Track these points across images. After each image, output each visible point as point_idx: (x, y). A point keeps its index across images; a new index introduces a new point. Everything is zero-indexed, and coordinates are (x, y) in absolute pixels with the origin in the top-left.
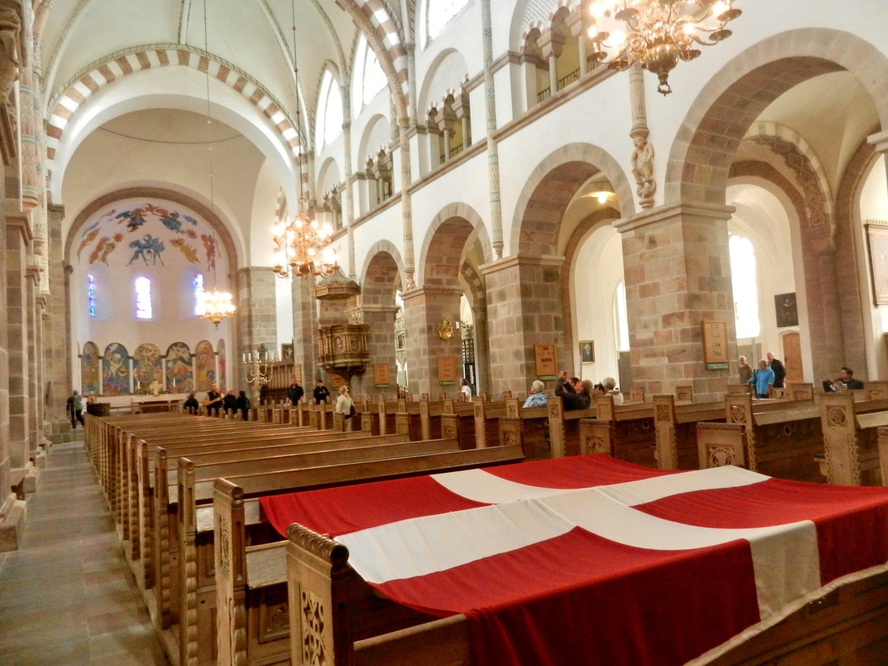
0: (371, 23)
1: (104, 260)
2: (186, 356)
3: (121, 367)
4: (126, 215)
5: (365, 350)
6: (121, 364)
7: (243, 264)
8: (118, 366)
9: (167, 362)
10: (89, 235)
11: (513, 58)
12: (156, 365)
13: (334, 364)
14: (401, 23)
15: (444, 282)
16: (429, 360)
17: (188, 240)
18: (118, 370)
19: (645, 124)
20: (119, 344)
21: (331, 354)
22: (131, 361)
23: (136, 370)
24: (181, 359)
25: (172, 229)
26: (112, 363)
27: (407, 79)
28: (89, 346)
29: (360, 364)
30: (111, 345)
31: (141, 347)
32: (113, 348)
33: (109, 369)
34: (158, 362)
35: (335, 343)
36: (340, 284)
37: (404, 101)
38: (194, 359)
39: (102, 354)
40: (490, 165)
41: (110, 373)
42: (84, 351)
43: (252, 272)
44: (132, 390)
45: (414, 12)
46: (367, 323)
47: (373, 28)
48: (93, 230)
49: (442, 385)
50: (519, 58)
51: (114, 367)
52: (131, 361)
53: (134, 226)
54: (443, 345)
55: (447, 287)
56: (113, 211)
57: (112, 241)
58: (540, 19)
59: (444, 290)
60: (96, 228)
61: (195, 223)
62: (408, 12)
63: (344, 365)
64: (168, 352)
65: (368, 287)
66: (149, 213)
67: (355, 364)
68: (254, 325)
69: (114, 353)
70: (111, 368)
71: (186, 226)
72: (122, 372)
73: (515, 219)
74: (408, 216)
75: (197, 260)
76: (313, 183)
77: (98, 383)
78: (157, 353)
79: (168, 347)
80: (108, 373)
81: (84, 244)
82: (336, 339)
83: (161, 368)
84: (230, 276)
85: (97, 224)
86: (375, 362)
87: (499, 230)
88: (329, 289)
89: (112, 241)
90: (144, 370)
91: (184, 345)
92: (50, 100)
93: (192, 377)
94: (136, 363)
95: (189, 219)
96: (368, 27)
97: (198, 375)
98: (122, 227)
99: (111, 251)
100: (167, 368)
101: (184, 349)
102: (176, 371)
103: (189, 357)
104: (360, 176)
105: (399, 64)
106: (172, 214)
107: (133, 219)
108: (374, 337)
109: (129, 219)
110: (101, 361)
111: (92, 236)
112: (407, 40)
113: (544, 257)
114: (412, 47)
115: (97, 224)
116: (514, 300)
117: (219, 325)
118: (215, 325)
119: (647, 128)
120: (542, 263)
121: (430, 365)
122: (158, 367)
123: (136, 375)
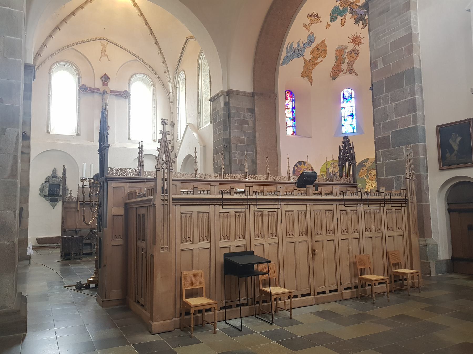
10: (312, 52)
26: (367, 181)
48: (313, 46)
57: (351, 47)
89: (351, 47)
99: (356, 58)
107: (352, 12)
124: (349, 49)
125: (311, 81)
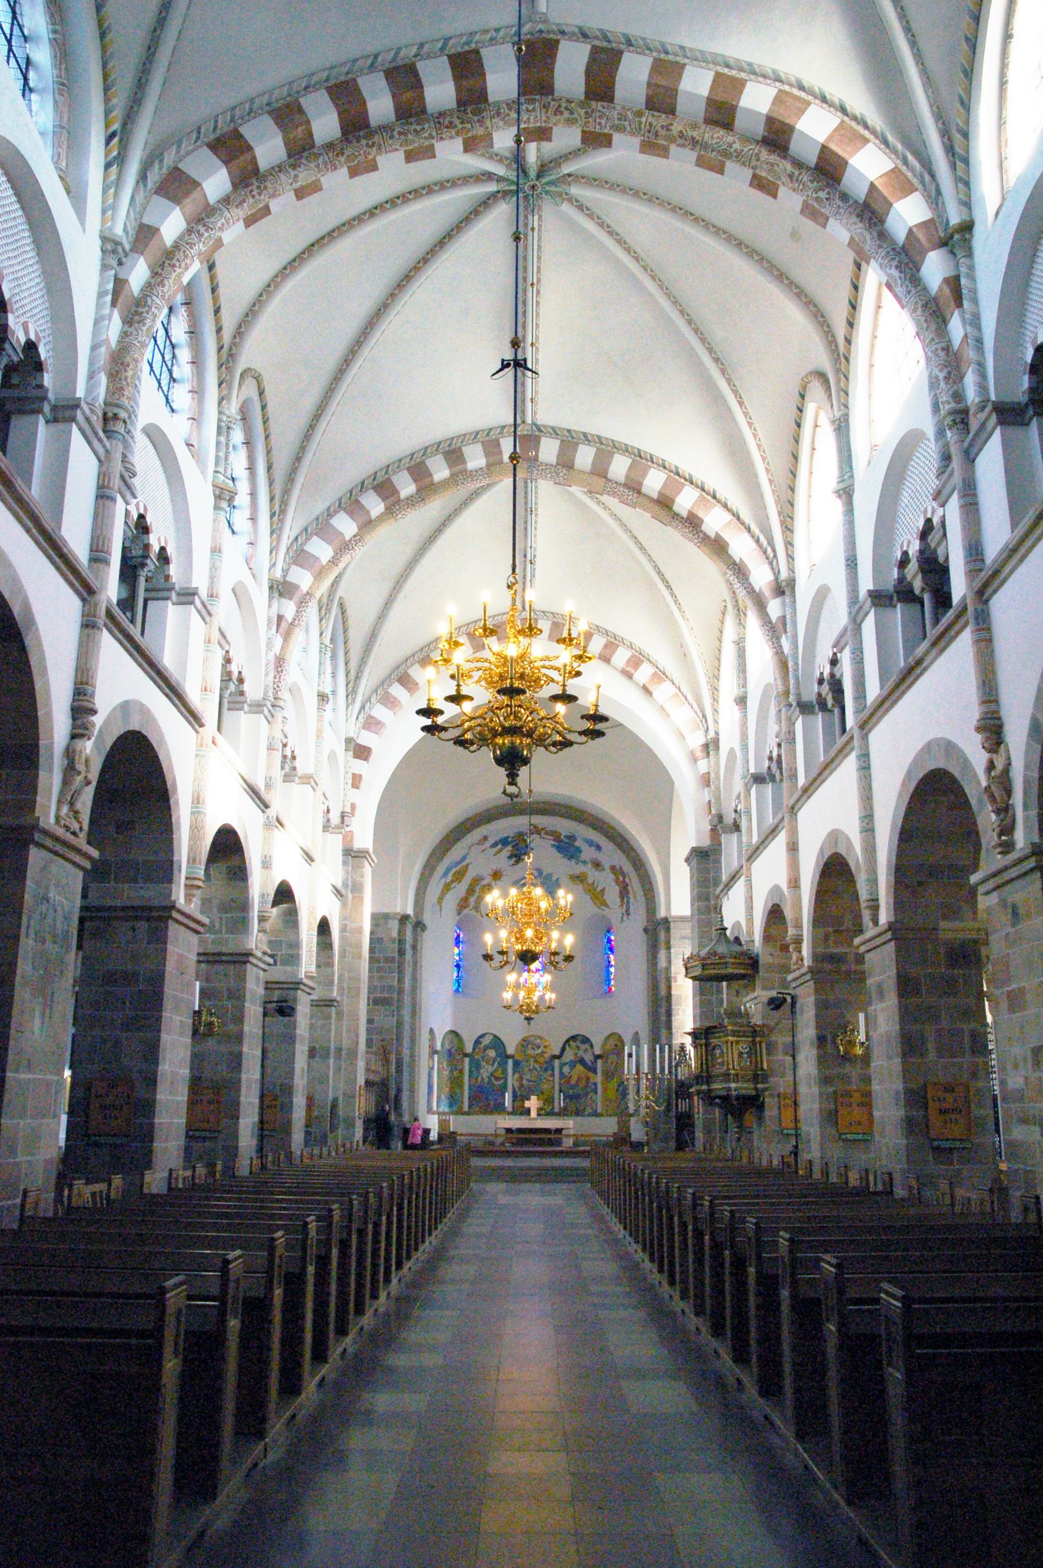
0: (730, 557)
1: (477, 908)
2: (588, 1058)
3: (495, 1071)
4: (504, 842)
5: (762, 1069)
6: (496, 1064)
7: (662, 913)
8: (491, 1069)
9: (562, 1065)
11: (879, 598)
12: (546, 1070)
13: (710, 1091)
14: (774, 551)
15: (851, 958)
16: (821, 1095)
17: (592, 875)
18: (492, 1075)
19: (997, 712)
20: (495, 1036)
21: (705, 1074)
22: (510, 1062)
23: (517, 1076)
24: (582, 1061)
25: (571, 858)
26: (483, 1063)
27: (785, 632)
28: (450, 1036)
29: (754, 1093)
30: (483, 1036)
31: (524, 1040)
32: (486, 1041)
33: (479, 1073)
34: (548, 1066)
35: (713, 1055)
36: (720, 958)
37: (783, 664)
38: (599, 1062)
39: (469, 1049)
40: (858, 770)
41: (480, 1079)
42: (442, 1045)
43: (672, 925)
44: (510, 1109)
45: (791, 531)
46: (766, 1022)
47: (735, 563)
48: (459, 867)
49: (847, 1140)
50: (891, 598)
51: (486, 1071)
52: (510, 1062)
53: (517, 857)
54: (848, 1068)
55: (853, 967)
56: (485, 838)
58: (910, 538)
59: (848, 973)
60: (464, 864)
61: (599, 848)
62: (783, 532)
63: (725, 1093)
64: (563, 1050)
65: (770, 960)
66: (535, 836)
67: (744, 1092)
68: (674, 1012)
69: (486, 1048)
70: (482, 1071)
71: (588, 853)
72: (497, 1079)
73: (889, 861)
74: (793, 848)
75: (606, 905)
76: (718, 788)
77: (462, 1093)
78: (547, 1050)
79: (564, 1040)
80: (476, 1079)
81: (447, 888)
82: (714, 1048)
83: (553, 1075)
84: (646, 930)
85: (464, 858)
86: (782, 1090)
87: (873, 881)
88: (704, 966)
90: (528, 1077)
91: (586, 1040)
92: (360, 712)
93: (596, 1093)
94: (517, 1064)
95: (591, 843)
96: (725, 563)
97: (605, 1090)
98: (502, 860)
100: (561, 1073)
101: (587, 1046)
102: (573, 1082)
103: (592, 1058)
104: (758, 779)
105: (775, 608)
106: (569, 837)
108: (780, 1046)
109: (509, 848)
110: (467, 1060)
111: (459, 876)
112: (784, 574)
113: (944, 924)
114: (792, 583)
115: (464, 858)
116: (892, 1000)
117: (532, 1022)
118: (526, 1022)
119: (999, 718)
120: (943, 935)
121: (820, 1103)
122: (550, 1072)
123: (517, 1084)
124: (485, 882)
125: (441, 910)
